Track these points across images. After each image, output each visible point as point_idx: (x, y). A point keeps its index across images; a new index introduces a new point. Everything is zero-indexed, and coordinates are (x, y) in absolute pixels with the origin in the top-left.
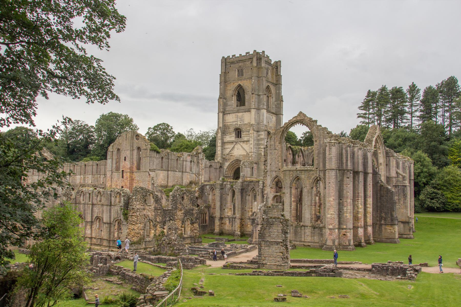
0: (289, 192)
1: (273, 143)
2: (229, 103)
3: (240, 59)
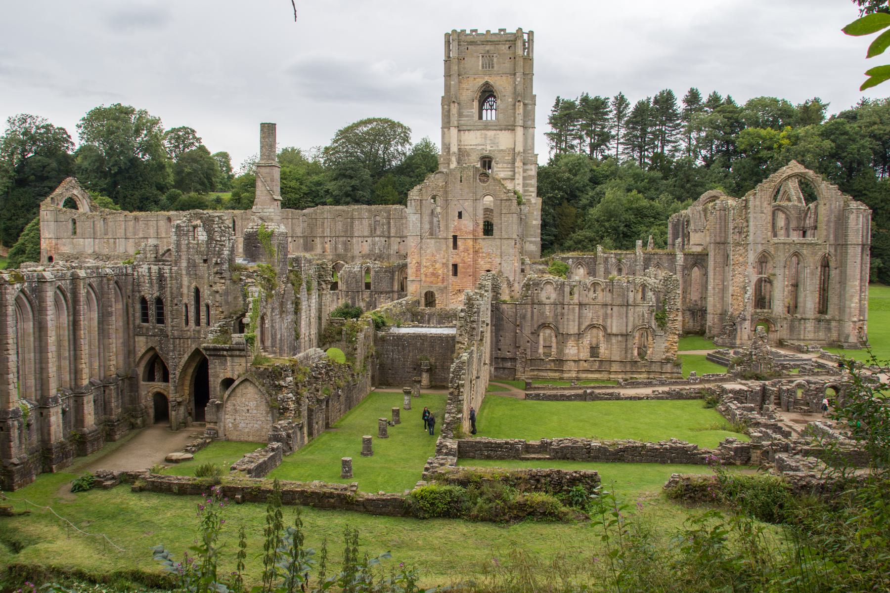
0: (782, 274)
1: (758, 203)
2: (465, 112)
3: (489, 38)
